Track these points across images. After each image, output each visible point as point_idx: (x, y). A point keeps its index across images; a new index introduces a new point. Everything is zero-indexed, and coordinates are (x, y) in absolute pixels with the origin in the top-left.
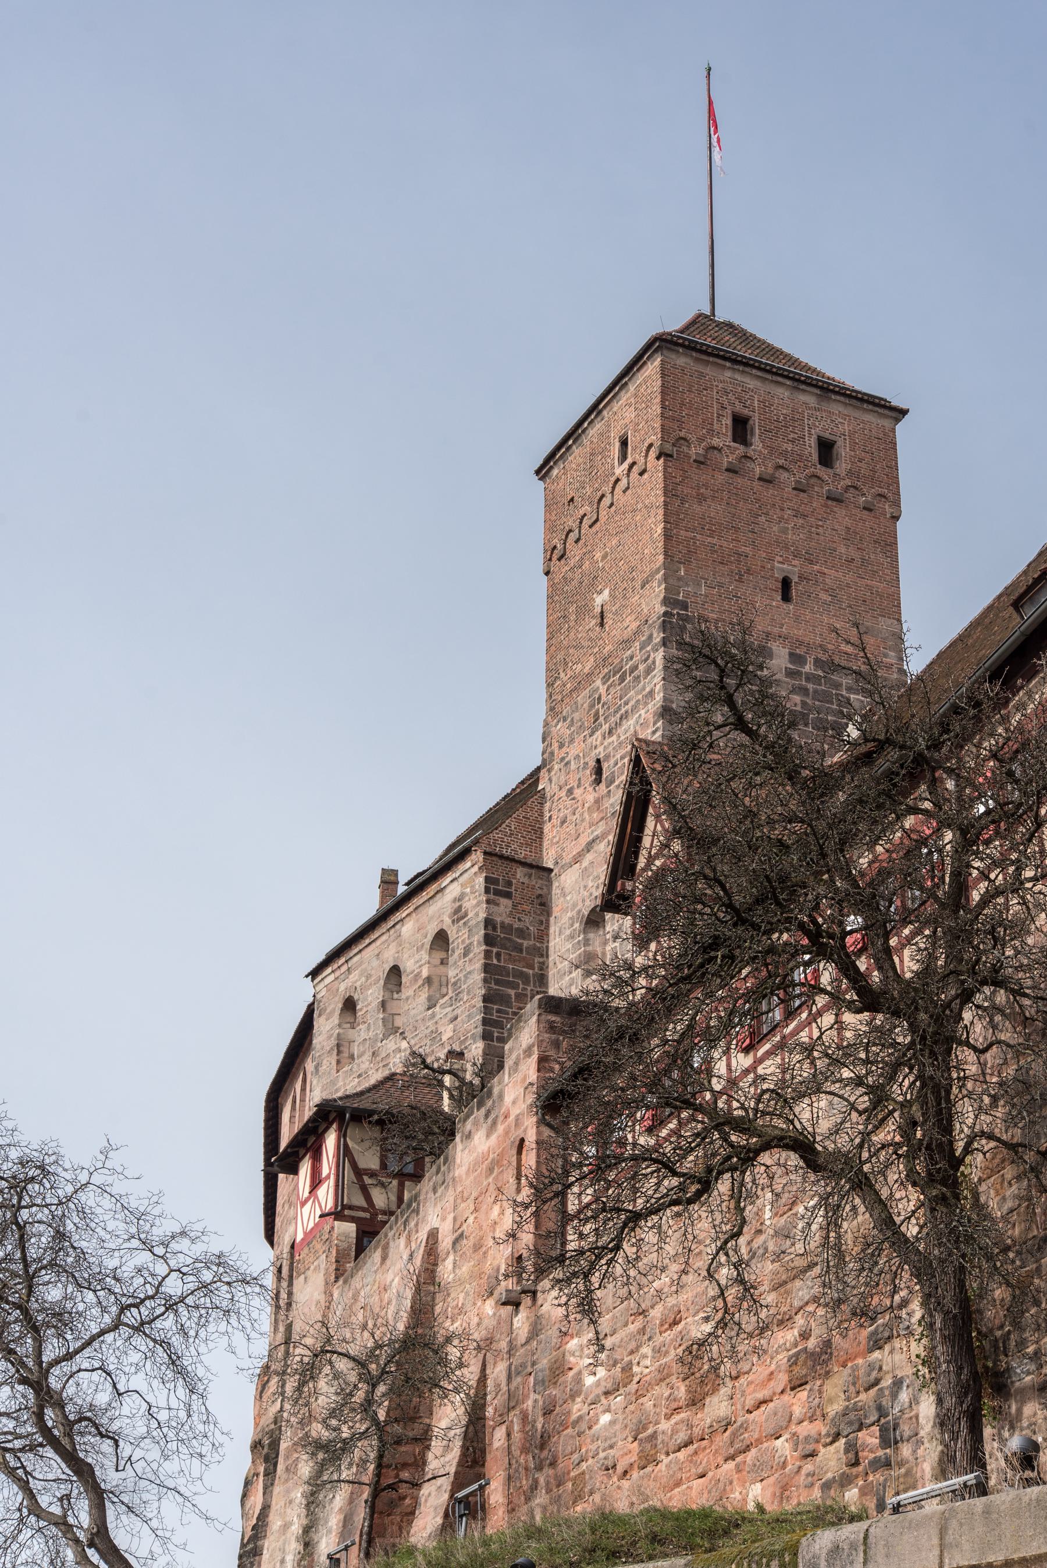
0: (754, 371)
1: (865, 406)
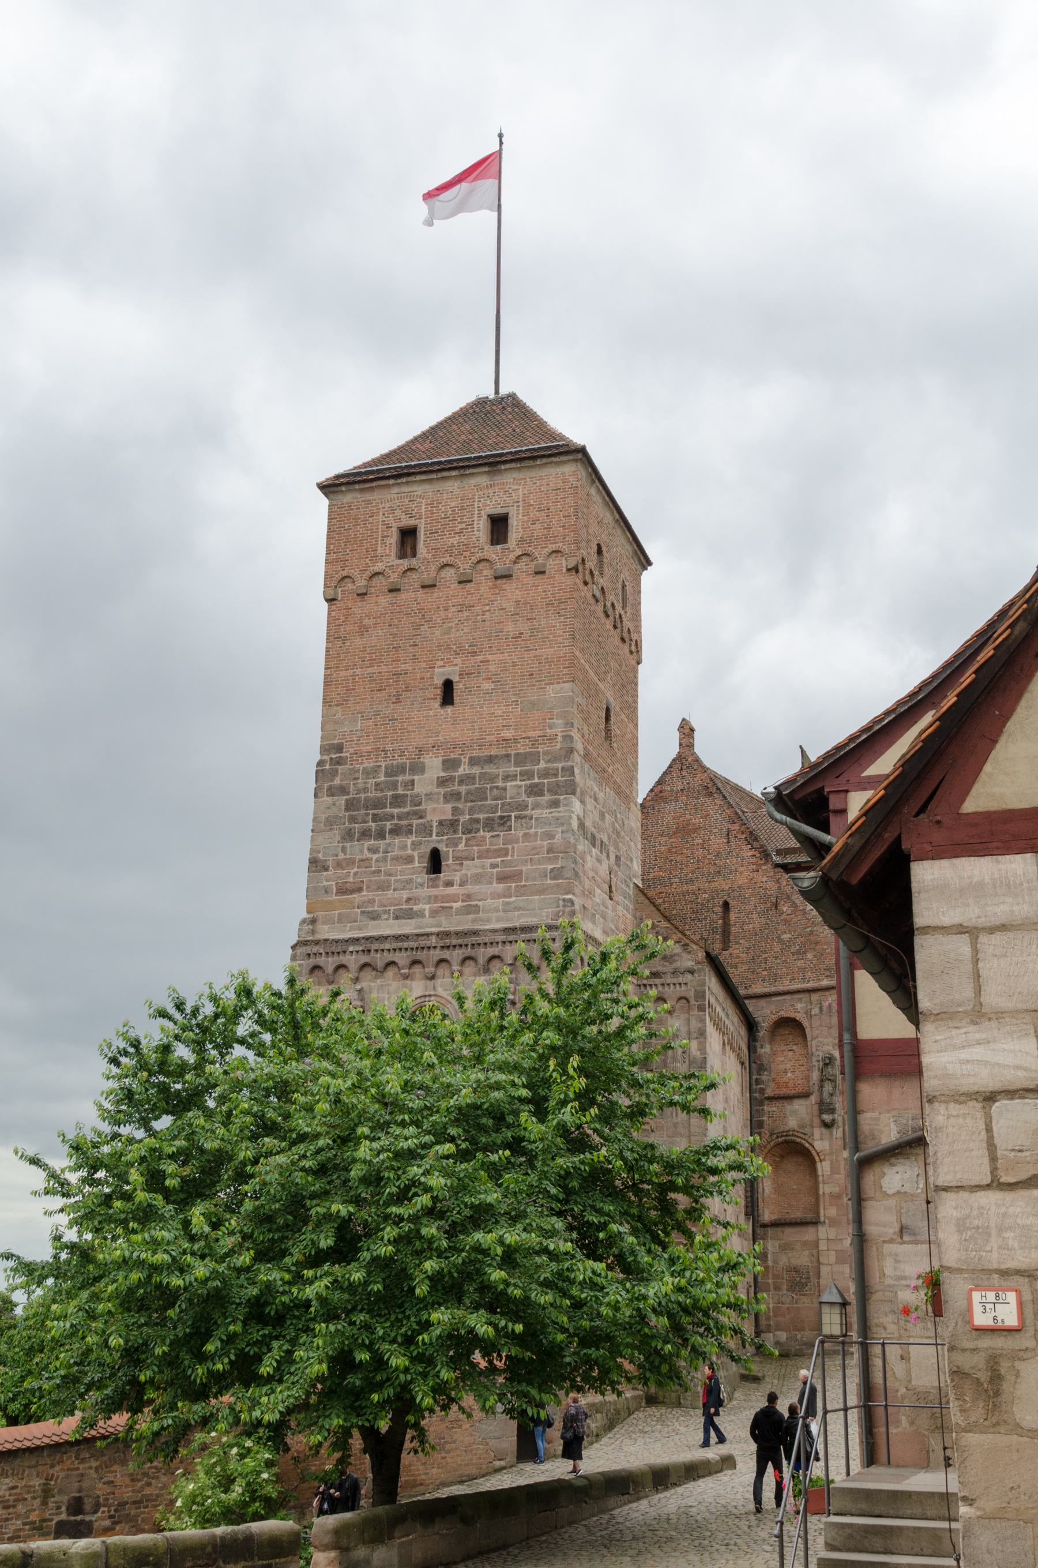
0: (419, 478)
1: (538, 462)
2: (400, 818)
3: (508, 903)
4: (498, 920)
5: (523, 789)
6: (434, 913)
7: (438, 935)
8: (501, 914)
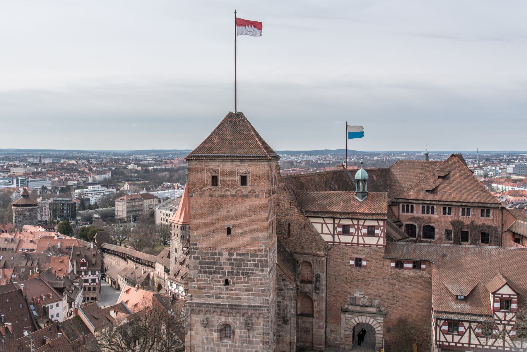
2: (216, 268)
3: (249, 298)
4: (246, 302)
5: (253, 265)
6: (227, 298)
7: (229, 305)
8: (247, 300)
